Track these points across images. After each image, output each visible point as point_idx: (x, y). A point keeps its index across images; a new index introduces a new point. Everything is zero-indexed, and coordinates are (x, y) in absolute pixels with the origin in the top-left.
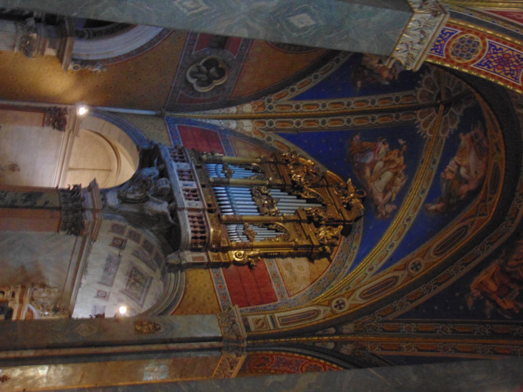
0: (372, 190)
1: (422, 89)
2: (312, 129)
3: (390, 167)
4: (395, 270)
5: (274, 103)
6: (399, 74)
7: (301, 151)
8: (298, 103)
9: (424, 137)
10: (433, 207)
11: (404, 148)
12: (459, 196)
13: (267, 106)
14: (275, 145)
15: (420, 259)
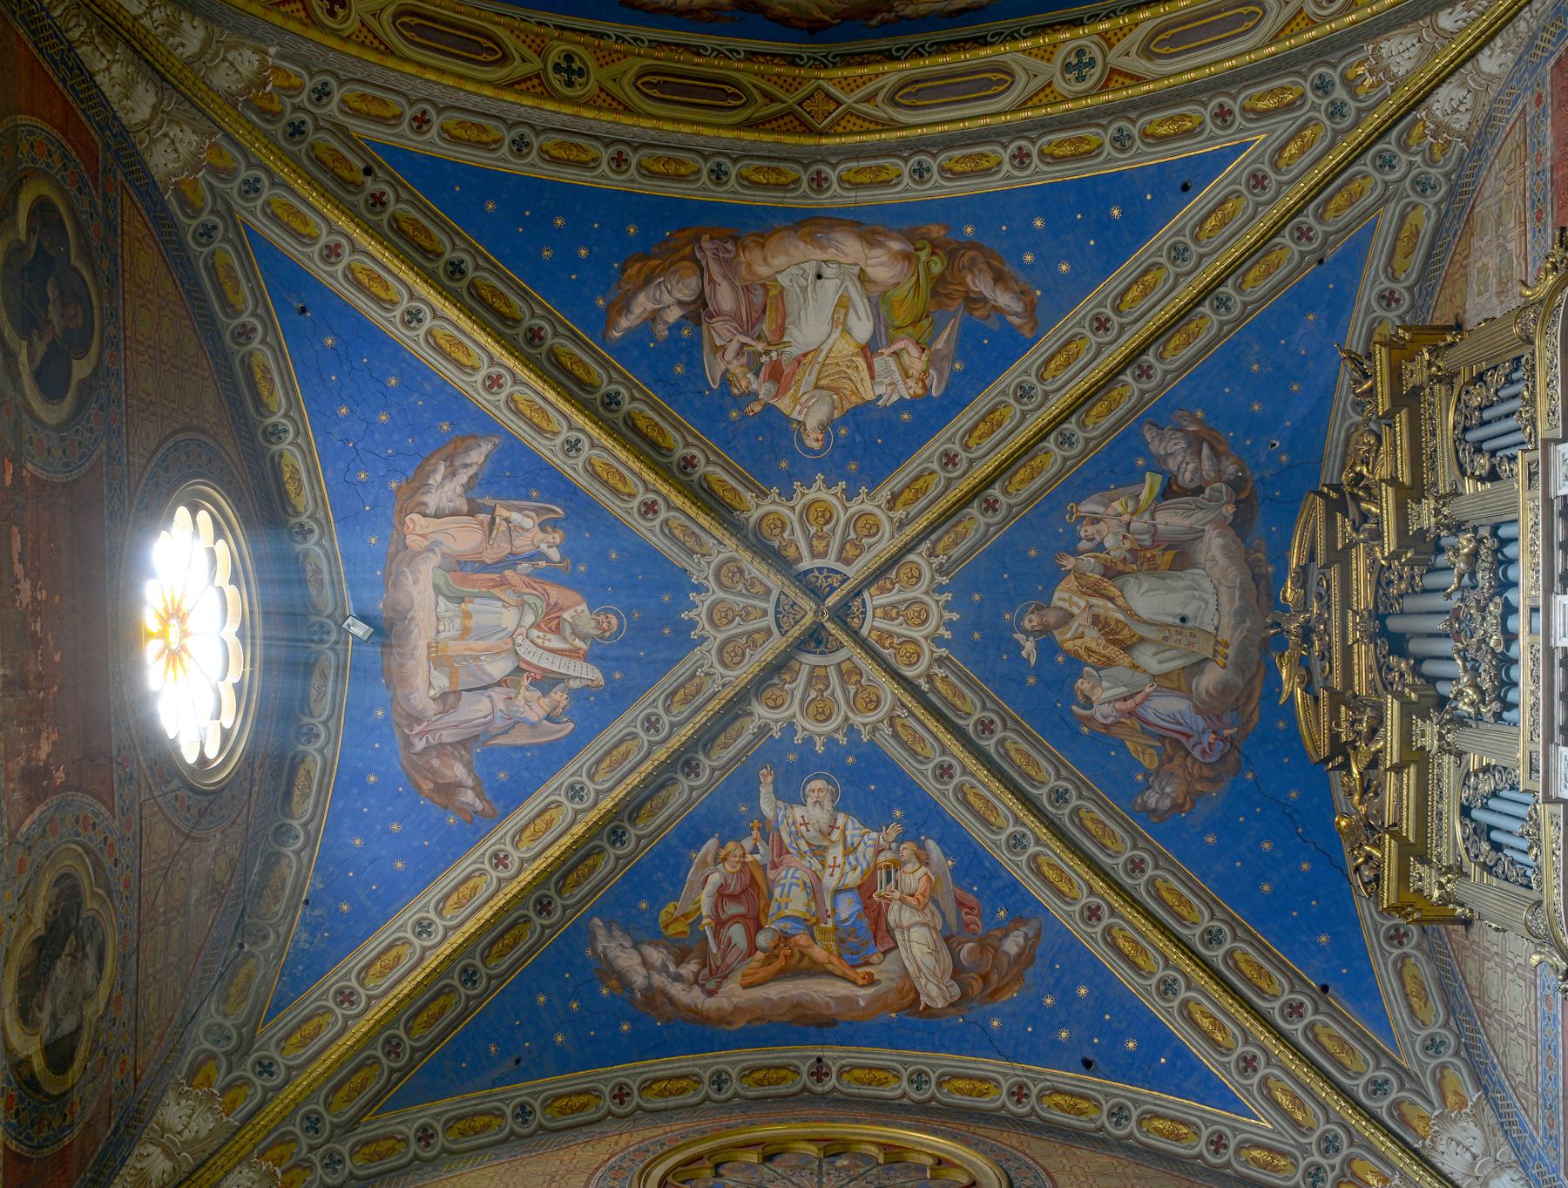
0: (1241, 614)
1: (851, 715)
2: (1263, 950)
3: (1120, 616)
4: (1139, 80)
5: (1305, 1151)
6: (879, 831)
7: (1367, 924)
8: (1231, 1081)
9: (945, 580)
10: (1004, 300)
11: (1031, 621)
12: (907, 257)
13: (1337, 1160)
14: (1435, 1011)
15: (1060, 85)
